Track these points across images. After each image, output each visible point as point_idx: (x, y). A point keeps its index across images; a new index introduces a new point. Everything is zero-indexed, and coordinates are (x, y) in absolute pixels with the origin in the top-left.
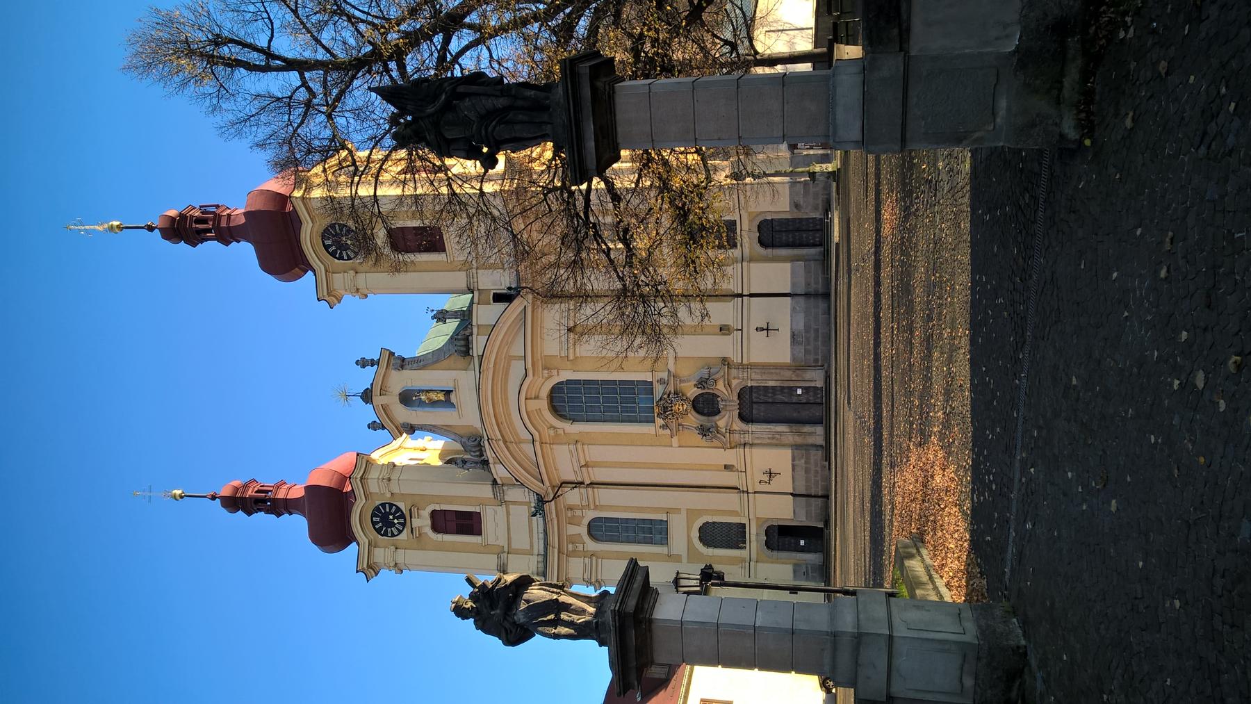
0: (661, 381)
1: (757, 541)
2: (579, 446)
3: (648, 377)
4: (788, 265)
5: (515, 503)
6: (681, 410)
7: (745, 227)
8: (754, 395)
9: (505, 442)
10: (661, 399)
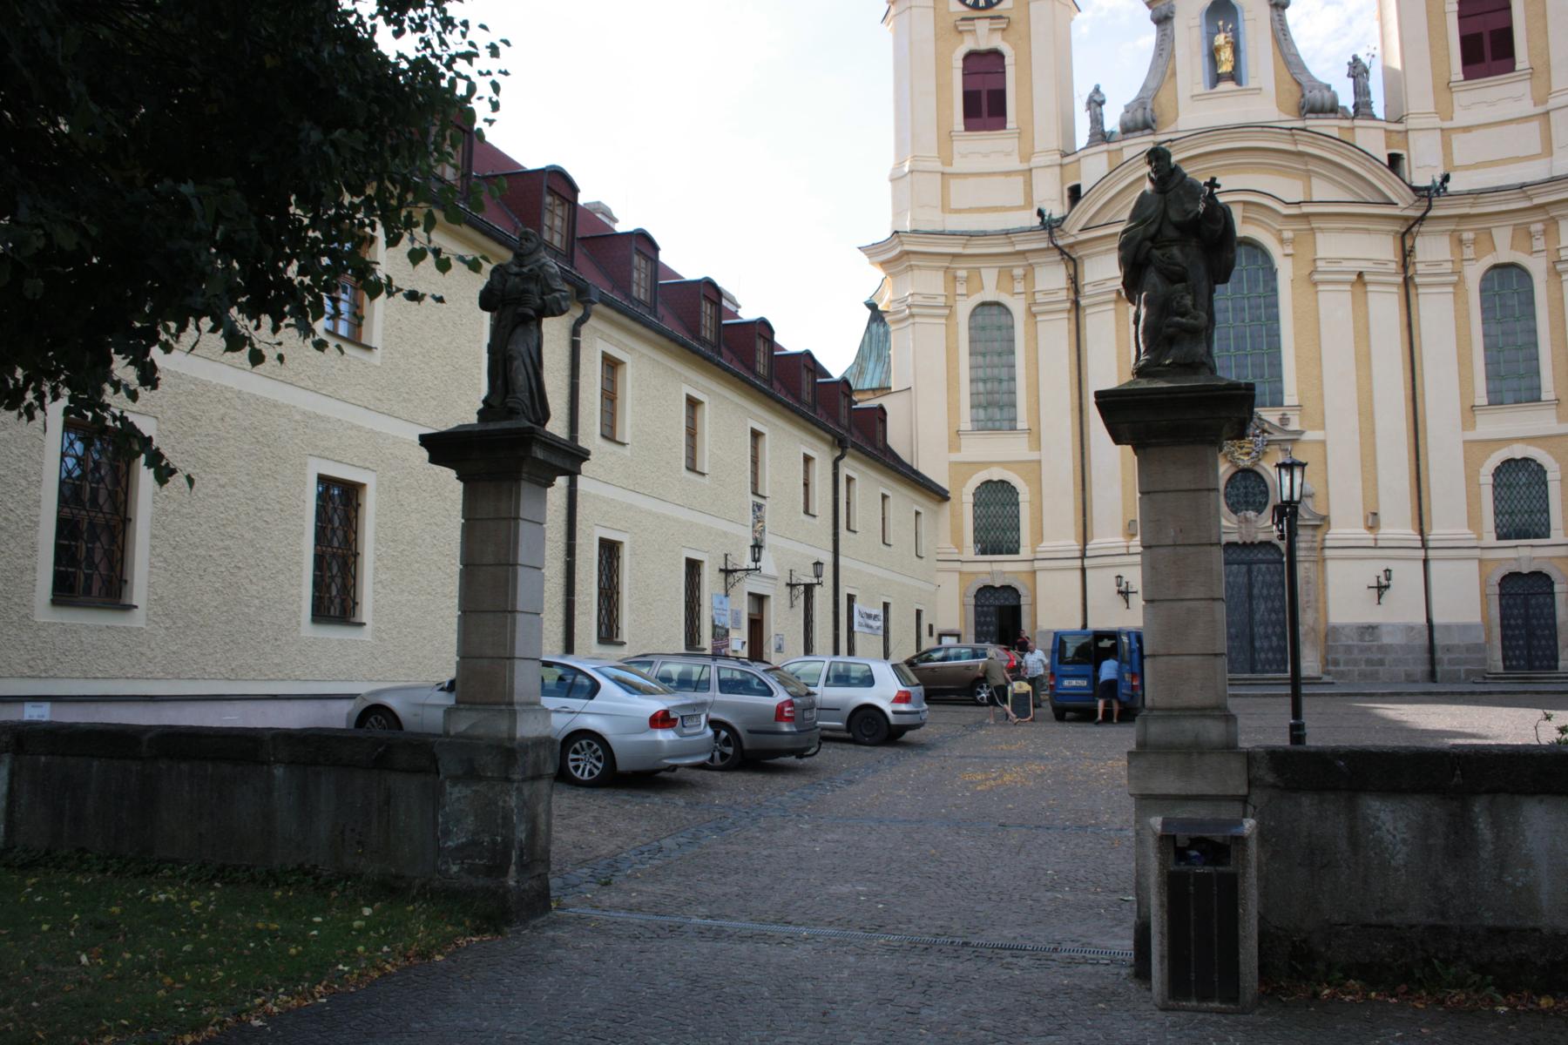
0: (1284, 420)
3: (1287, 401)
5: (1029, 186)
8: (1263, 567)
10: (1260, 419)
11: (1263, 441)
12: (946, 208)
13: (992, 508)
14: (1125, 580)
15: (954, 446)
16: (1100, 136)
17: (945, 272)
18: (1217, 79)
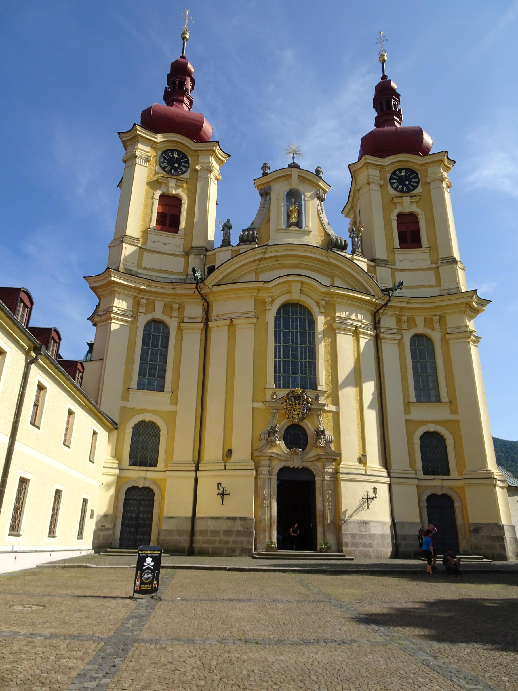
0: (317, 398)
1: (139, 478)
2: (254, 320)
3: (320, 388)
4: (418, 520)
5: (187, 262)
6: (294, 413)
7: (446, 483)
9: (260, 260)
11: (307, 408)
12: (139, 266)
13: (143, 437)
14: (222, 486)
15: (126, 397)
16: (226, 243)
17: (134, 298)
18: (290, 225)
